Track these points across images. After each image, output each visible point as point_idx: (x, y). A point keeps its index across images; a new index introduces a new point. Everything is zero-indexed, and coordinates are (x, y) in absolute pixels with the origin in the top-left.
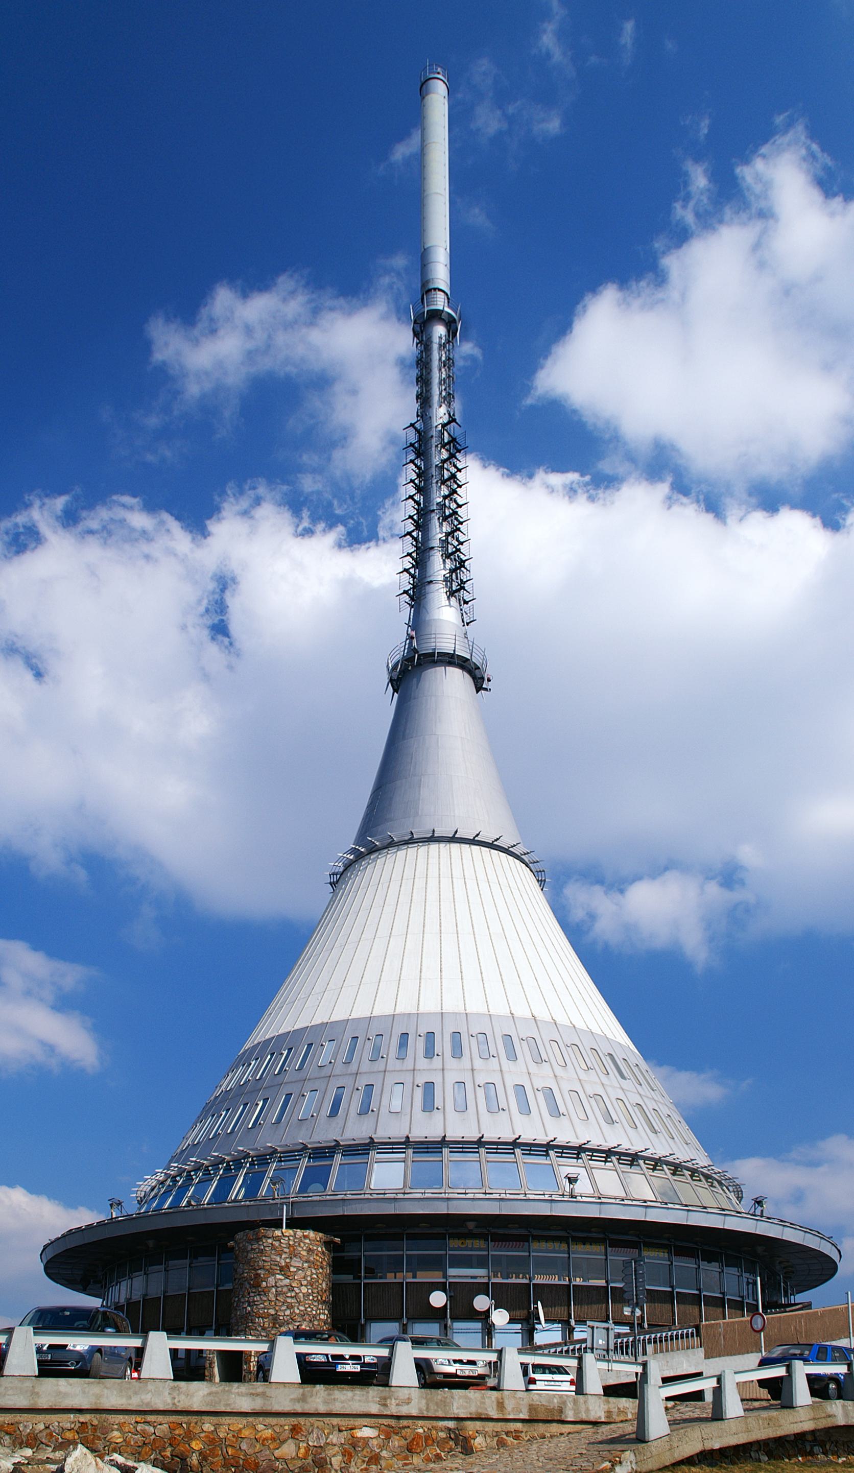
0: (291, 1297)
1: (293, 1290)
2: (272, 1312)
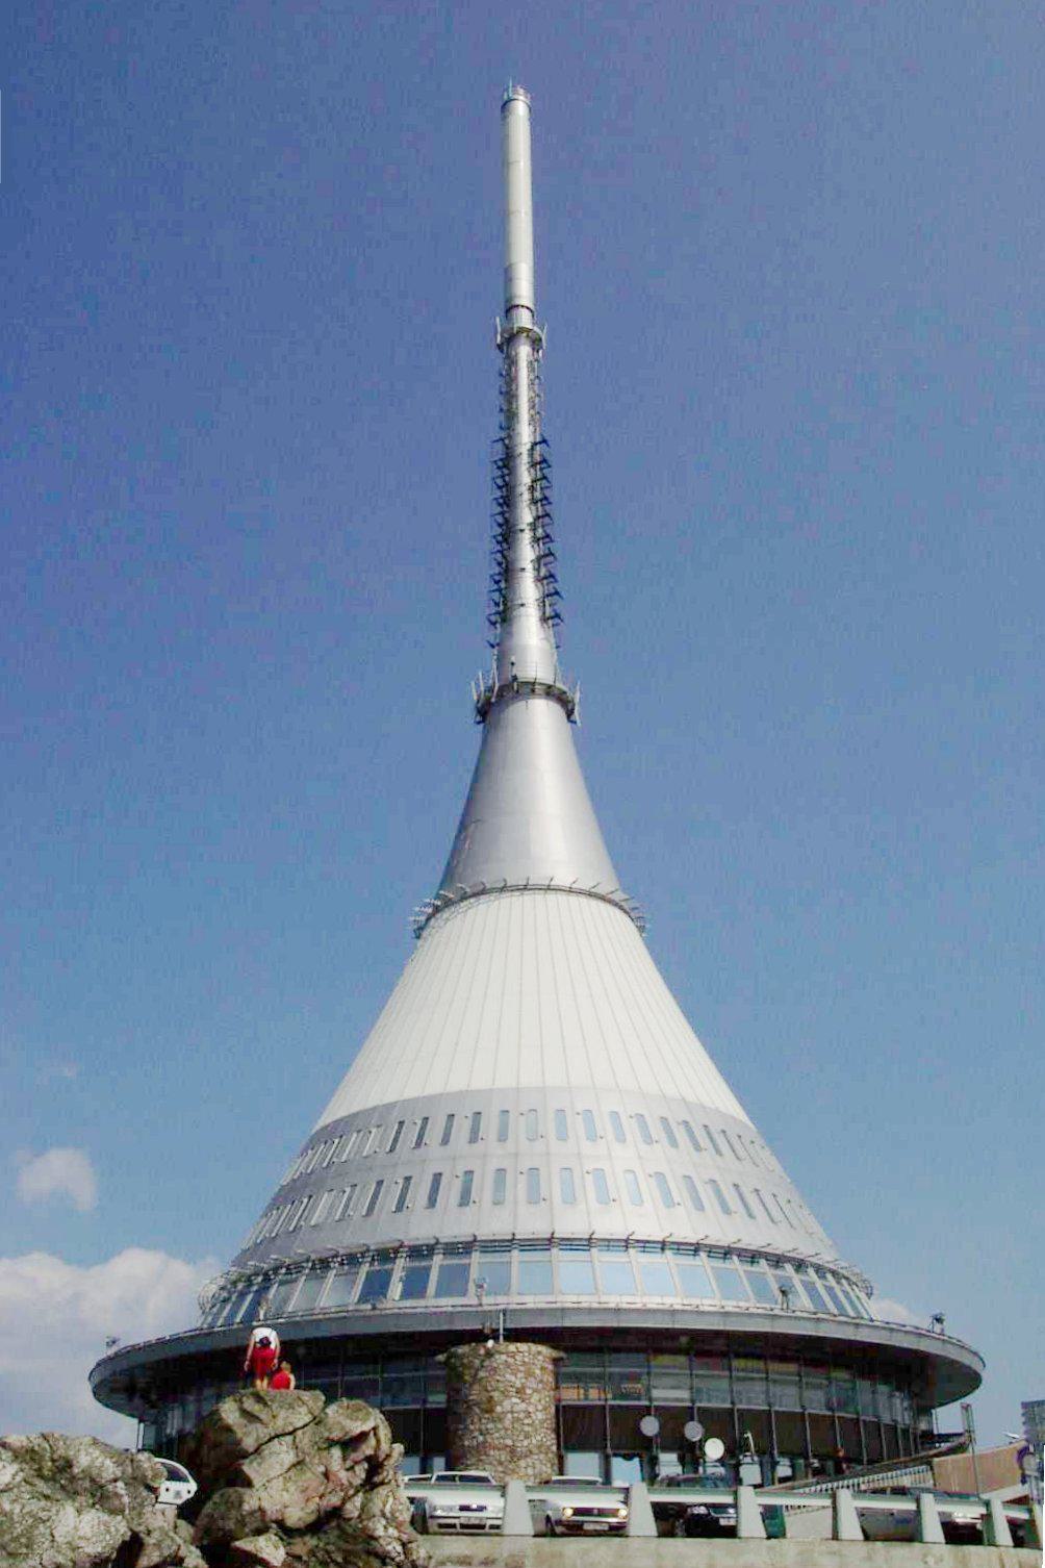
0: (528, 1424)
2: (509, 1442)
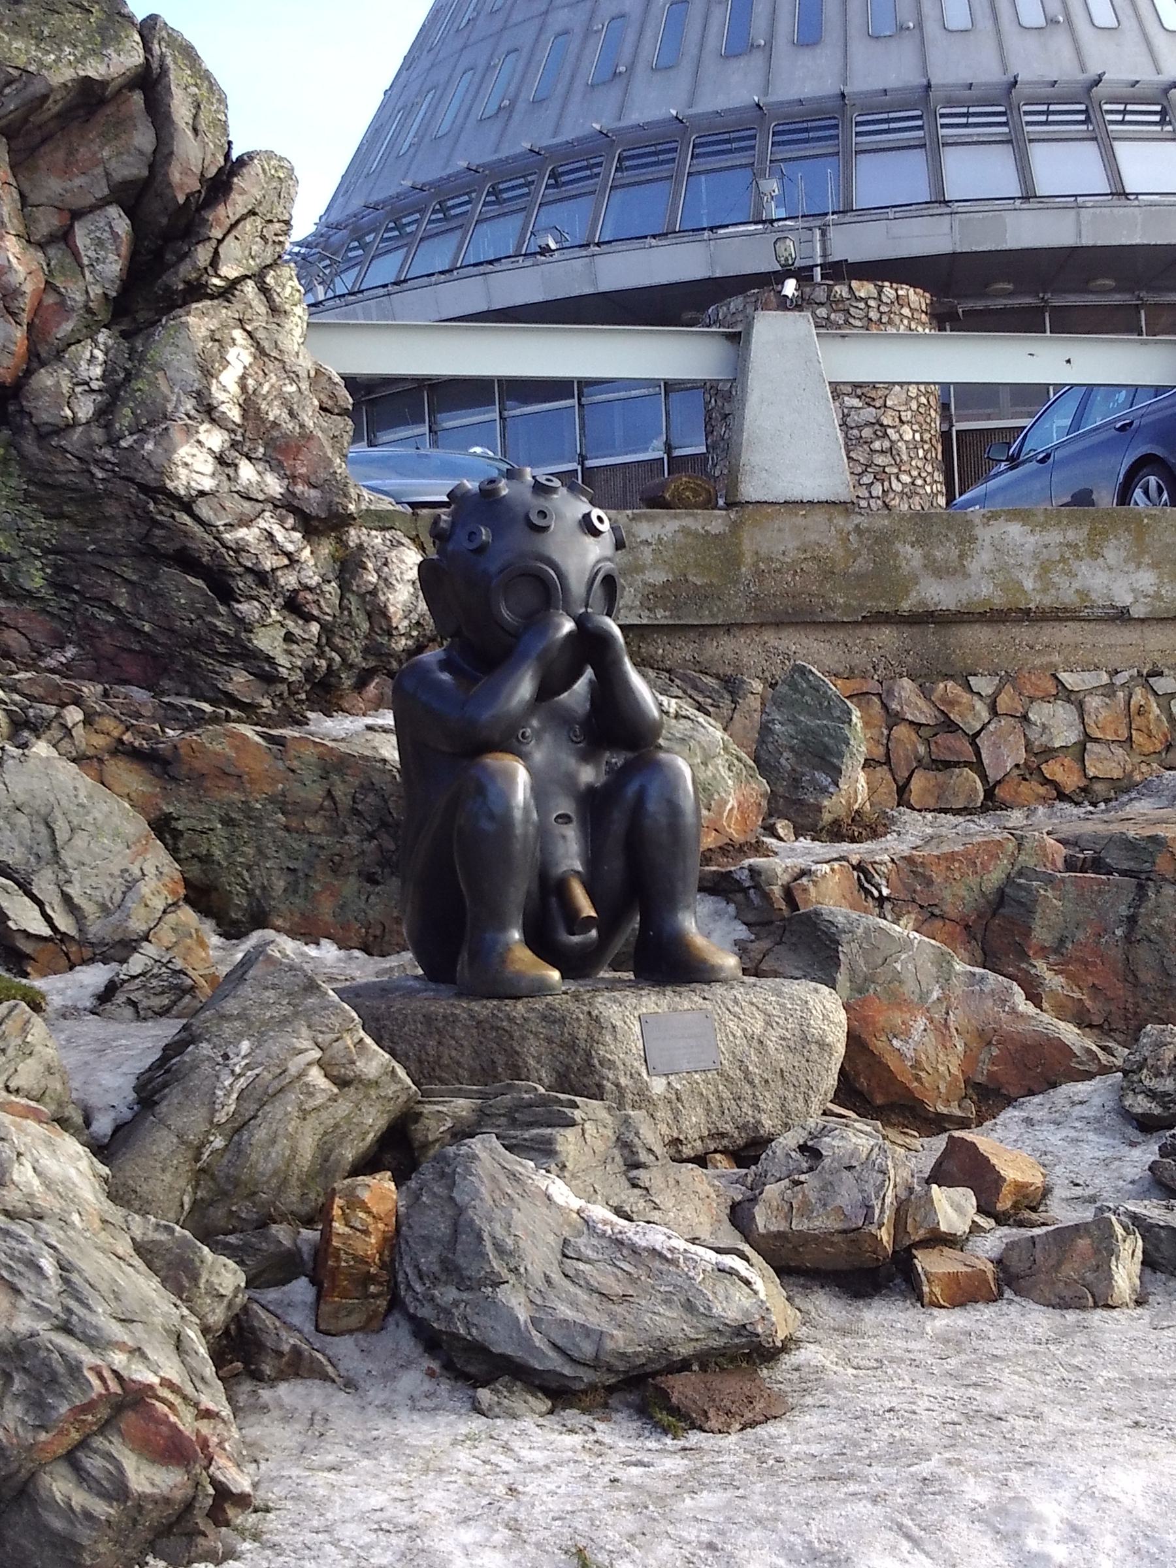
1: (886, 435)
